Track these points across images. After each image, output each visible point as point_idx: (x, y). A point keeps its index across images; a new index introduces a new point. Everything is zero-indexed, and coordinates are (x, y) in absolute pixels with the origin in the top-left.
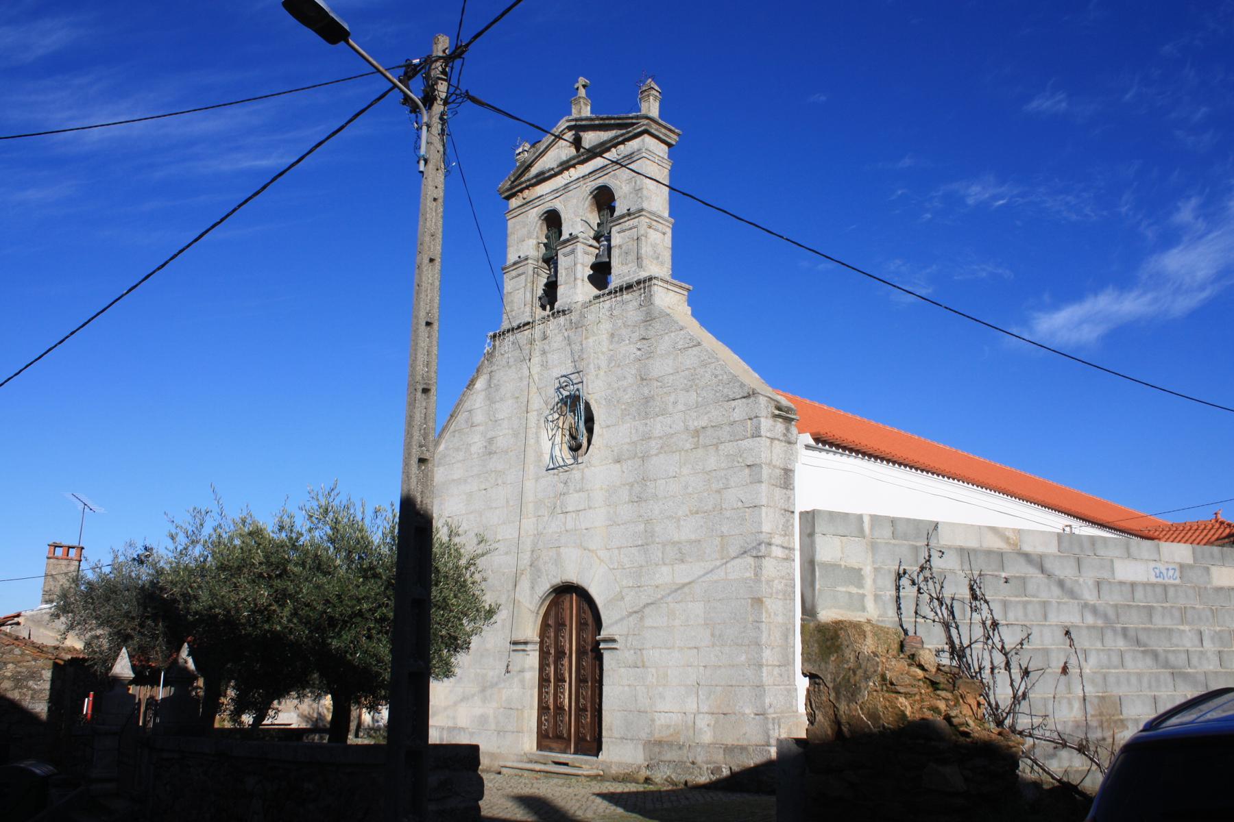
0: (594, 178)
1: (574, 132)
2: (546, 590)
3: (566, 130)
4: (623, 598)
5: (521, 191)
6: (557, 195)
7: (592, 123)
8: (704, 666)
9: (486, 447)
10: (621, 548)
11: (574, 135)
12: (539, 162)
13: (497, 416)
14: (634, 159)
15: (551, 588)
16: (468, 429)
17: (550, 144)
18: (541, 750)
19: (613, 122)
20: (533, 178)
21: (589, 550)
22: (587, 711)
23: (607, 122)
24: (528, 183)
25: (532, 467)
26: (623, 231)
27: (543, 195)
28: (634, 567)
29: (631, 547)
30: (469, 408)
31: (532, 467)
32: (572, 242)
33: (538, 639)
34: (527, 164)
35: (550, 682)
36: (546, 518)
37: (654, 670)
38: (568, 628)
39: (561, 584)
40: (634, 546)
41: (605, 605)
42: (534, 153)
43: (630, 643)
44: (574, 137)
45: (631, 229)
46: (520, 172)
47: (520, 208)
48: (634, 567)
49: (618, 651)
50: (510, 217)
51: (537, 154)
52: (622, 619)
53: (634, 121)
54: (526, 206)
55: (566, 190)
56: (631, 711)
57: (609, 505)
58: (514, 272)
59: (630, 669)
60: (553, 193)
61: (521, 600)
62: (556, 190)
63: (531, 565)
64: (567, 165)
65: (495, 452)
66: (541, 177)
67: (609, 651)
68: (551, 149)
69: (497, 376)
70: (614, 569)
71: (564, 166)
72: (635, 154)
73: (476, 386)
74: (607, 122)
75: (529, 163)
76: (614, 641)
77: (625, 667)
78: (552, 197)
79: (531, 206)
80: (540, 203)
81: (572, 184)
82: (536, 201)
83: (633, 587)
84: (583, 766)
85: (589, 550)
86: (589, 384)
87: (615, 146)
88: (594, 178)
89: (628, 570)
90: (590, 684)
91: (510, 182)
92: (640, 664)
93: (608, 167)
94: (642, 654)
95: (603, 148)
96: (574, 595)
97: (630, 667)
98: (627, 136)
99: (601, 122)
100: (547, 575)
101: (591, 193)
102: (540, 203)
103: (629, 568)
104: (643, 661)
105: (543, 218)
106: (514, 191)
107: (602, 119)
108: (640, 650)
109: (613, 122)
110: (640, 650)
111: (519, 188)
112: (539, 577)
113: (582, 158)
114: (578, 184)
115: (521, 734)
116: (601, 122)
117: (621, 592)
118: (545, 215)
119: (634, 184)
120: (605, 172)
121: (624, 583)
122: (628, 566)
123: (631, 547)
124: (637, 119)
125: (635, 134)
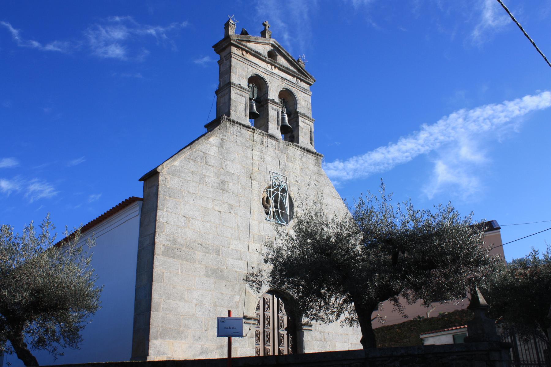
0: (287, 83)
1: (273, 49)
3: (270, 44)
5: (243, 49)
6: (266, 73)
7: (288, 56)
8: (351, 343)
9: (219, 184)
11: (272, 49)
12: (252, 44)
13: (228, 169)
14: (307, 93)
16: (203, 164)
17: (262, 43)
19: (298, 66)
20: (253, 51)
23: (295, 64)
24: (249, 50)
25: (256, 214)
26: (304, 123)
27: (258, 65)
30: (204, 151)
31: (256, 214)
32: (278, 105)
34: (249, 39)
37: (330, 343)
42: (255, 39)
44: (271, 50)
45: (308, 124)
46: (244, 39)
47: (242, 58)
49: (312, 332)
50: (234, 57)
51: (256, 41)
53: (308, 76)
54: (246, 60)
55: (271, 75)
58: (239, 91)
60: (264, 69)
62: (267, 70)
64: (273, 63)
65: (227, 191)
66: (258, 55)
67: (307, 331)
68: (261, 45)
69: (227, 145)
71: (272, 63)
72: (308, 91)
73: (209, 140)
74: (295, 64)
75: (251, 40)
77: (316, 340)
78: (263, 71)
79: (249, 64)
80: (255, 67)
81: (275, 75)
82: (253, 64)
86: (291, 186)
87: (297, 78)
88: (287, 83)
91: (237, 39)
92: (323, 340)
93: (295, 85)
94: (324, 334)
95: (293, 74)
97: (318, 341)
98: (305, 79)
99: (293, 61)
101: (284, 88)
102: (254, 66)
104: (325, 338)
105: (253, 75)
106: (240, 45)
107: (293, 59)
108: (323, 332)
109: (298, 66)
110: (323, 332)
111: (244, 48)
113: (282, 68)
114: (279, 79)
116: (292, 60)
118: (255, 75)
119: (306, 104)
120: (293, 86)
124: (310, 77)
125: (308, 82)
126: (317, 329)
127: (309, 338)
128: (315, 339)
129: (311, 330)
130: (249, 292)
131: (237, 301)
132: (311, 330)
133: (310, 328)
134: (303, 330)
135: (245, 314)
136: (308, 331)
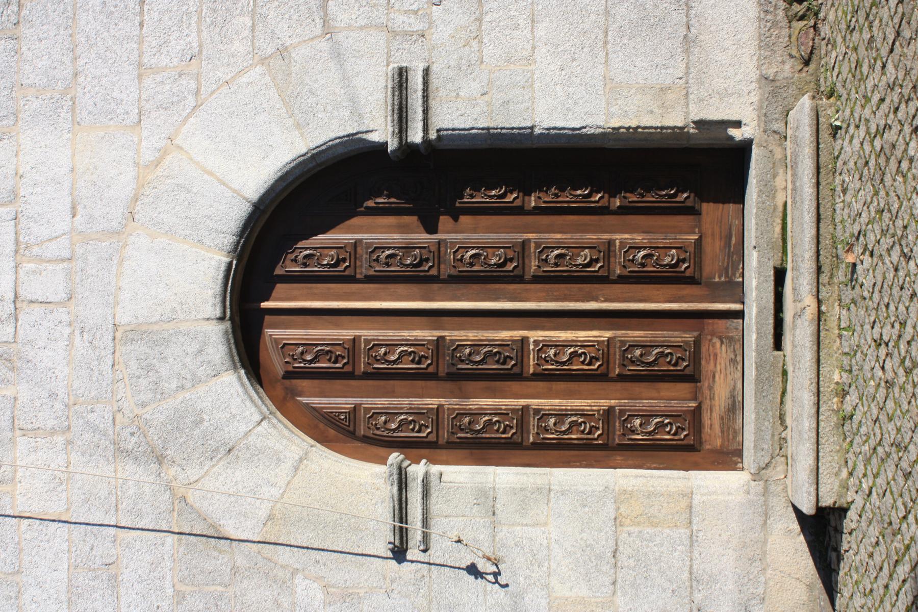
2: (240, 390)
4: (283, 52)
10: (140, 65)
15: (235, 368)
18: (739, 453)
21: (136, 199)
22: (610, 243)
28: (199, 11)
29: (141, 25)
33: (395, 457)
35: (525, 409)
36: (24, 392)
38: (368, 332)
39: (228, 325)
40: (141, 13)
41: (298, 126)
43: (412, 19)
48: (199, 11)
49: (434, 68)
52: (337, 55)
56: (607, 12)
57: (16, 114)
59: (488, 18)
61: (263, 511)
63: (160, 460)
67: (433, 103)
70: (198, 91)
76: (402, 77)
83: (253, 14)
84: (780, 199)
85: (136, 199)
89: (205, 33)
90: (530, 236)
96: (265, 305)
97: (479, 20)
100: (196, 381)
103: (199, 32)
112: (198, 422)
115: (697, 499)
117: (263, 60)
121: (240, 47)
122: (193, 38)
123: (141, 25)
126: (418, 26)
127: (471, 87)
128: (474, 44)
129: (426, 72)
130: (270, 518)
131: (320, 596)
132: (426, 72)
133: (416, 81)
134: (433, 135)
135: (383, 549)
136: (431, 95)
